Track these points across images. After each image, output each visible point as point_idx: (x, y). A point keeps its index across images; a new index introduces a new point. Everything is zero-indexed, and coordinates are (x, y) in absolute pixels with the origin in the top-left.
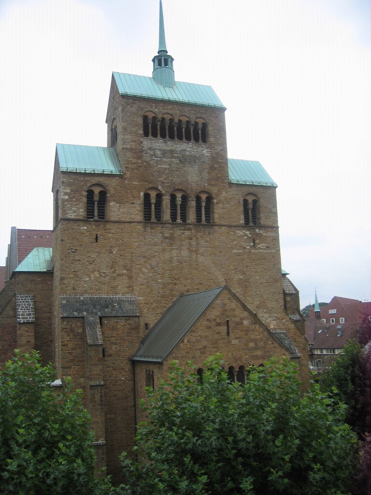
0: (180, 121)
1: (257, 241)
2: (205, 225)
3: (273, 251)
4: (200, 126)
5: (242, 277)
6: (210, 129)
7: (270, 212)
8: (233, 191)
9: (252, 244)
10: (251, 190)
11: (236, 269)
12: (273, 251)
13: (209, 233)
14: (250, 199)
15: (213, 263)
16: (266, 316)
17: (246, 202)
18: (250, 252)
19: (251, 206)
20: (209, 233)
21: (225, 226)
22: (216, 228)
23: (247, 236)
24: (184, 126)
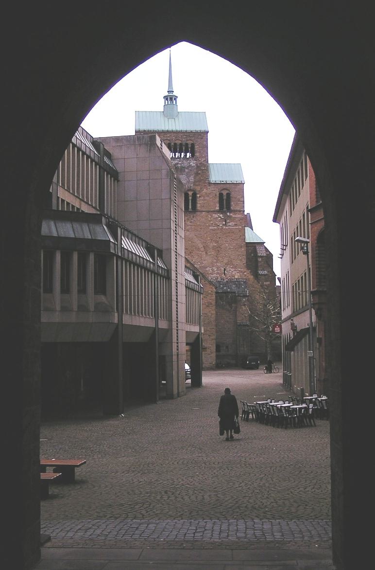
0: (175, 144)
1: (228, 221)
2: (191, 211)
3: (240, 227)
4: (190, 146)
5: (216, 245)
6: (196, 147)
7: (239, 201)
8: (212, 188)
9: (224, 223)
10: (225, 187)
11: (212, 239)
12: (240, 227)
13: (193, 217)
14: (225, 193)
15: (195, 235)
16: (232, 270)
17: (221, 195)
18: (222, 228)
19: (225, 197)
20: (193, 217)
21: (204, 211)
22: (198, 213)
23: (221, 218)
24: (178, 147)
